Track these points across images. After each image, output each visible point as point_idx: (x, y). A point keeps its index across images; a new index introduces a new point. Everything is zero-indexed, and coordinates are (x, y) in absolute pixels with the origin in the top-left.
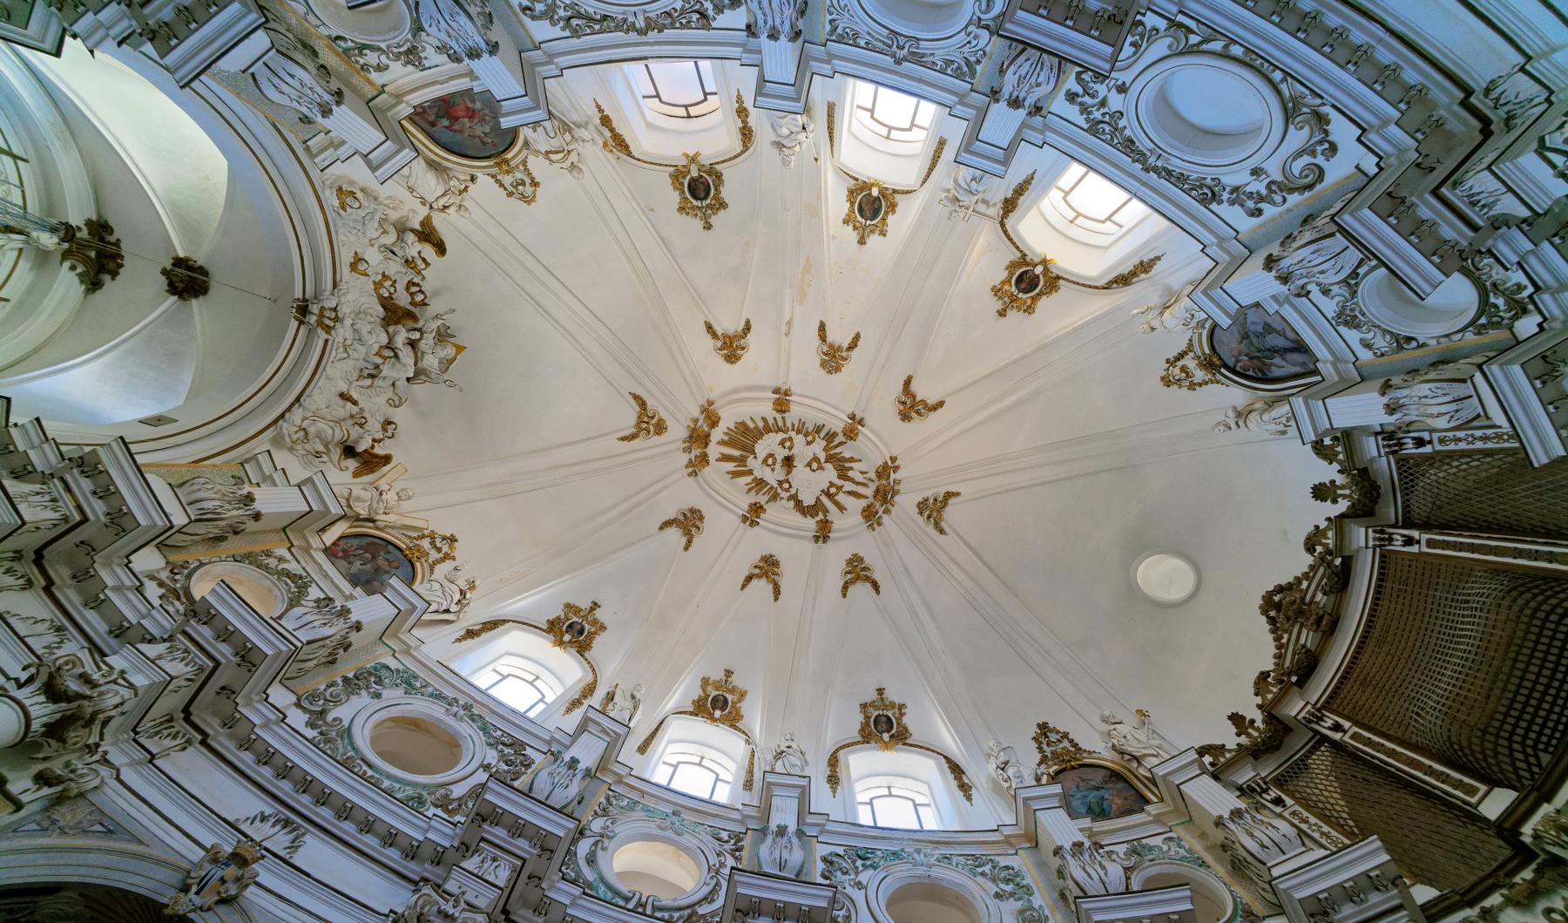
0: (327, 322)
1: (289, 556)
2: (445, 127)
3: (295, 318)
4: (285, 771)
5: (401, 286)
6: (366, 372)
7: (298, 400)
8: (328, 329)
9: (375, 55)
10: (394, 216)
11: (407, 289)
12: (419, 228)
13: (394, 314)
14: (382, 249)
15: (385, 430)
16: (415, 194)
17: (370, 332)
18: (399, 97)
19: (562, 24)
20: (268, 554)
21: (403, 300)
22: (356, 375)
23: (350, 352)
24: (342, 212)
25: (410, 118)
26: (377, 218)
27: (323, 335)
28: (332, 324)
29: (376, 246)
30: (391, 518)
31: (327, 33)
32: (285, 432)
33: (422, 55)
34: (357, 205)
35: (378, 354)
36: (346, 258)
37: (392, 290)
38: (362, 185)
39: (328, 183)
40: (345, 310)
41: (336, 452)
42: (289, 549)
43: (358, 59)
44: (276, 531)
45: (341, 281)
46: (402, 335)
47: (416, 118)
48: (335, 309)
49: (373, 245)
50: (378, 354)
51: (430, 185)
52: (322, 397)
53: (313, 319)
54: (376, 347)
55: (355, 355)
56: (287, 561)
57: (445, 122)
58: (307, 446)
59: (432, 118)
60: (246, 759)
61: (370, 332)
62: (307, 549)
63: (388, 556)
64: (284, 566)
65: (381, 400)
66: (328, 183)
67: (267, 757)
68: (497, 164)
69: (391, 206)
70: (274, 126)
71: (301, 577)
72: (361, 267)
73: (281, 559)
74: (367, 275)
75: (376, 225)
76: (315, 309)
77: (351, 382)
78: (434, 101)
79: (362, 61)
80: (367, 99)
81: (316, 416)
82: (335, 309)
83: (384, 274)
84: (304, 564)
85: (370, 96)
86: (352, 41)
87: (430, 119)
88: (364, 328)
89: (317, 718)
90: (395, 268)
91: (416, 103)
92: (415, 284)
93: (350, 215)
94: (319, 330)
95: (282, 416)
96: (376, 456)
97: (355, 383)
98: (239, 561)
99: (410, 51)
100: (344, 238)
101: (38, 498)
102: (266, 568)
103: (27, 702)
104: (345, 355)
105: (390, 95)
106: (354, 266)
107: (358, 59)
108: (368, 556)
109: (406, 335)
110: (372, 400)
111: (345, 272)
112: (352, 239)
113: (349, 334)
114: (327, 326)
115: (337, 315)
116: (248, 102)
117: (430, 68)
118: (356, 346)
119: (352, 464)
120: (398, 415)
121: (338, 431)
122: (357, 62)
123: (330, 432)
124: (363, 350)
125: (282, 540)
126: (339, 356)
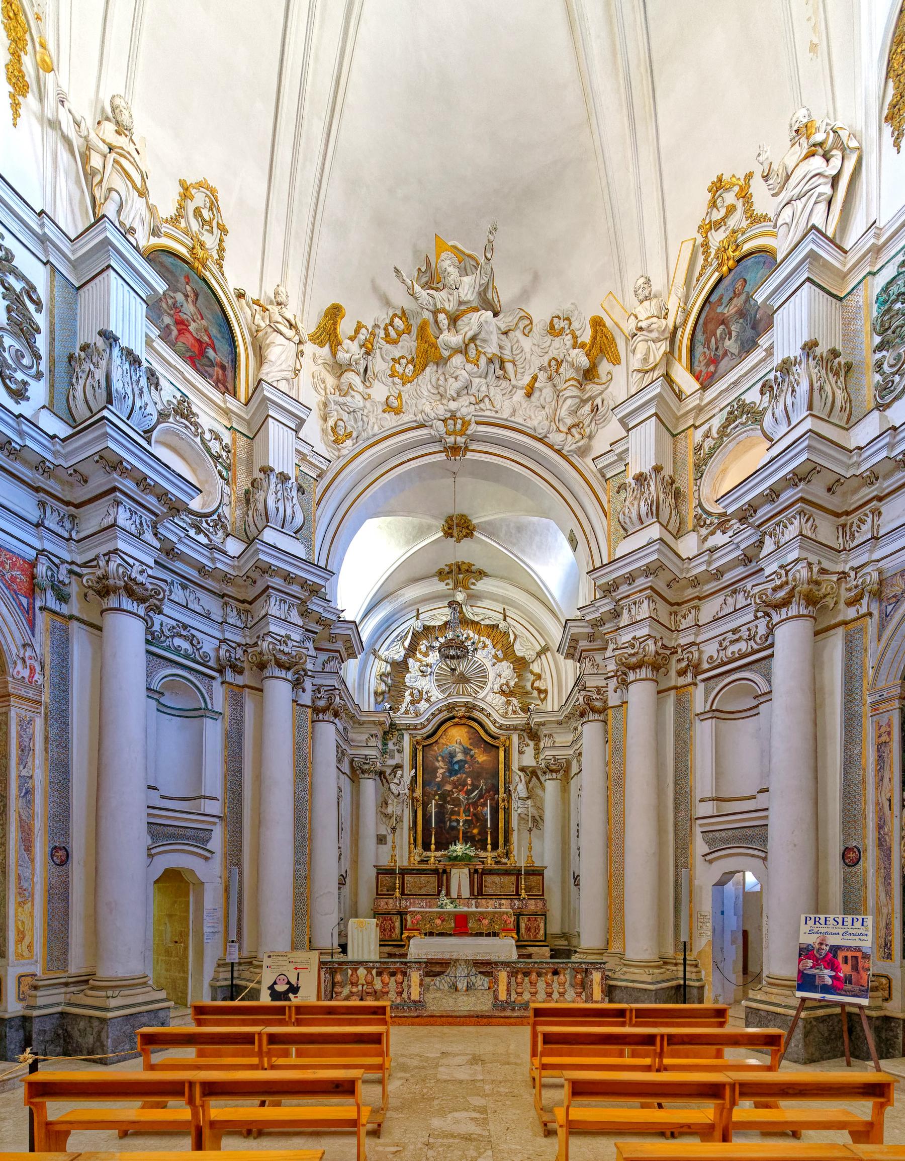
6: (499, 372)
17: (456, 378)
23: (482, 395)
24: (354, 435)
28: (459, 421)
45: (416, 421)
54: (469, 367)
61: (456, 378)
70: (318, 504)
77: (514, 387)
88: (453, 386)
97: (514, 382)
100: (376, 428)
104: (486, 400)
112: (372, 420)
113: (464, 401)
118: (473, 390)
126: (489, 407)
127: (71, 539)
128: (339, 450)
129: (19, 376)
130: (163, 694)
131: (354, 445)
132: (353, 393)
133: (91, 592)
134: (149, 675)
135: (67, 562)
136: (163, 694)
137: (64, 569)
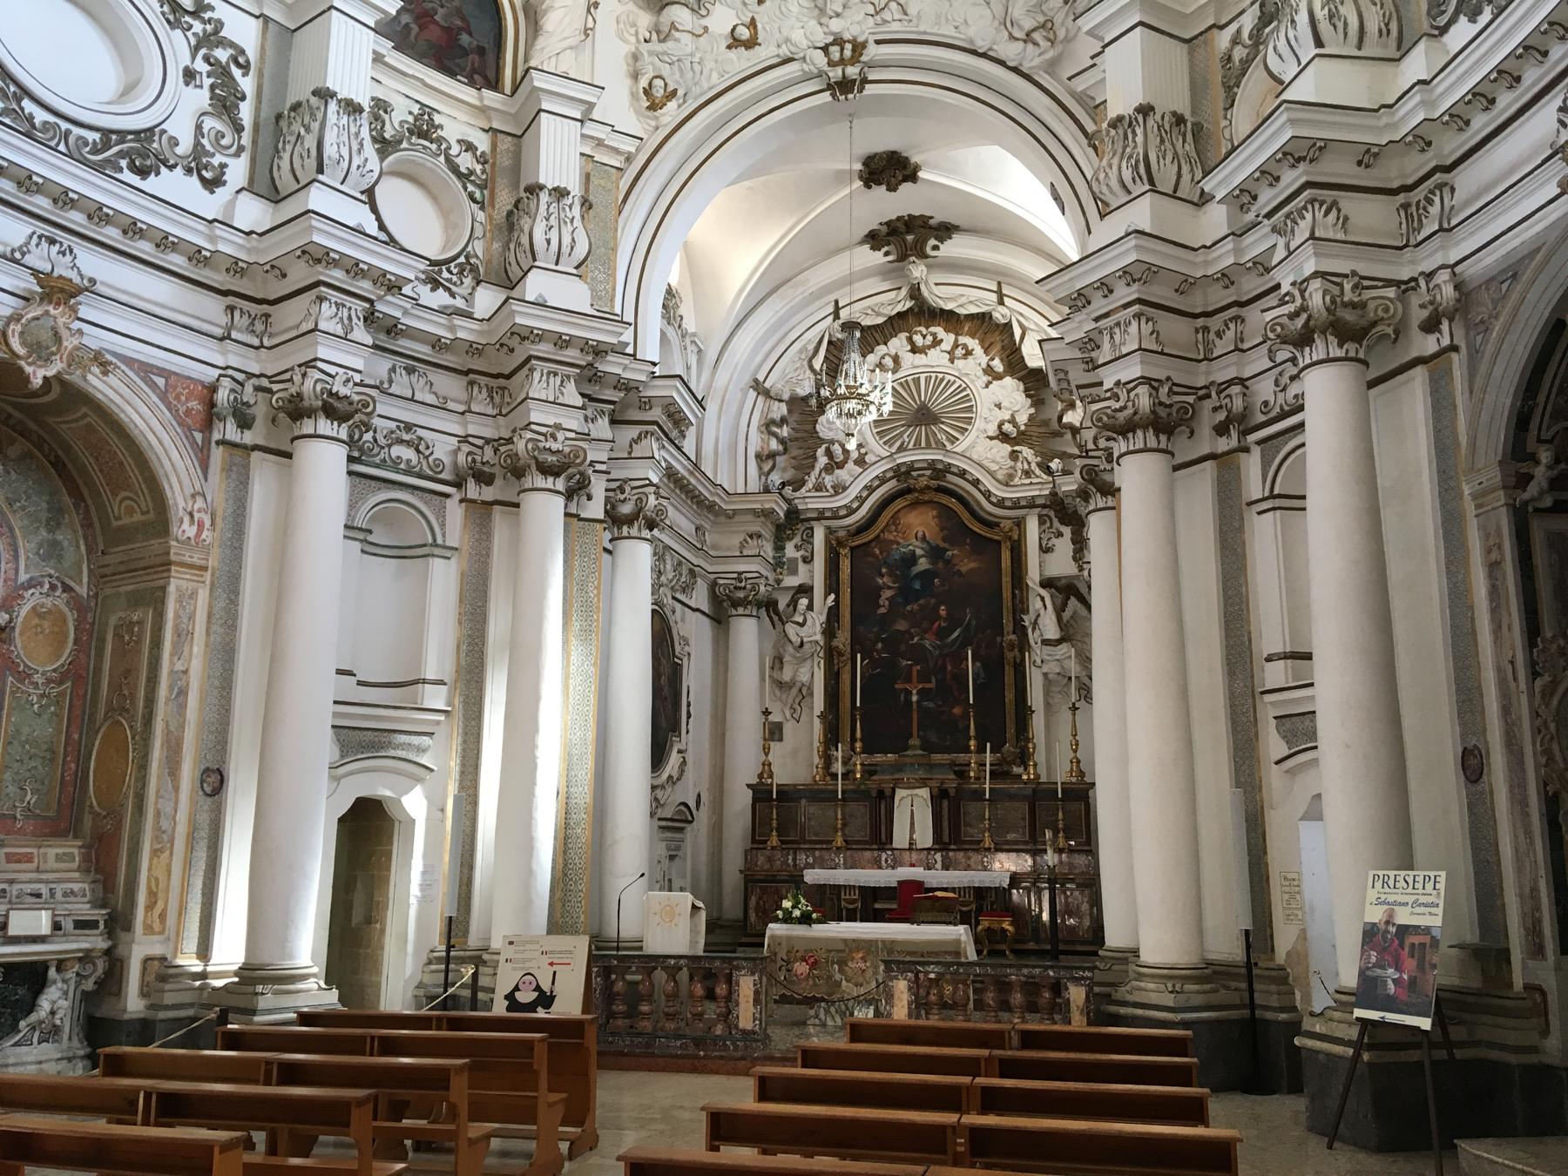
0: (848, 53)
1: (1233, 28)
2: (470, 34)
3: (861, 90)
7: (984, 55)
8: (858, 48)
9: (458, 160)
14: (703, 12)
16: (590, 24)
18: (483, 110)
19: (207, 15)
20: (1229, 58)
24: (680, 93)
25: (495, 85)
26: (659, 47)
27: (872, 52)
28: (849, 47)
29: (705, 22)
31: (481, 213)
32: (1037, 61)
33: (411, 119)
36: (742, 61)
38: (628, 82)
39: (653, 123)
42: (1222, 27)
43: (479, 172)
44: (1191, 53)
45: (778, 56)
47: (491, 74)
48: (825, 49)
49: (706, 29)
53: (852, 71)
56: (1239, 31)
57: (465, 39)
58: (1058, 20)
59: (474, 58)
60: (1482, 123)
64: (1245, 34)
66: (653, 123)
69: (633, 31)
72: (744, 33)
73: (1236, 40)
74: (753, 21)
75: (670, 44)
76: (836, 74)
78: (451, 73)
79: (478, 168)
80: (515, 140)
82: (825, 49)
85: (510, 139)
86: (465, 189)
87: (477, 58)
91: (473, 91)
93: (677, 82)
94: (864, 58)
95: (1015, 70)
98: (1233, 101)
99: (423, 135)
100: (715, 75)
101: (1117, 337)
103: (1308, 361)
105: (489, 119)
106: (751, 44)
107: (479, 172)
111: (765, 53)
112: (709, 64)
114: (853, 50)
115: (832, 44)
116: (615, 237)
117: (417, 101)
122: (483, 172)
125: (1205, 43)
127: (262, 346)
128: (657, 118)
129: (216, 160)
130: (370, 532)
131: (679, 106)
132: (677, 35)
133: (281, 415)
134: (353, 506)
135: (254, 375)
136: (370, 532)
137: (249, 388)
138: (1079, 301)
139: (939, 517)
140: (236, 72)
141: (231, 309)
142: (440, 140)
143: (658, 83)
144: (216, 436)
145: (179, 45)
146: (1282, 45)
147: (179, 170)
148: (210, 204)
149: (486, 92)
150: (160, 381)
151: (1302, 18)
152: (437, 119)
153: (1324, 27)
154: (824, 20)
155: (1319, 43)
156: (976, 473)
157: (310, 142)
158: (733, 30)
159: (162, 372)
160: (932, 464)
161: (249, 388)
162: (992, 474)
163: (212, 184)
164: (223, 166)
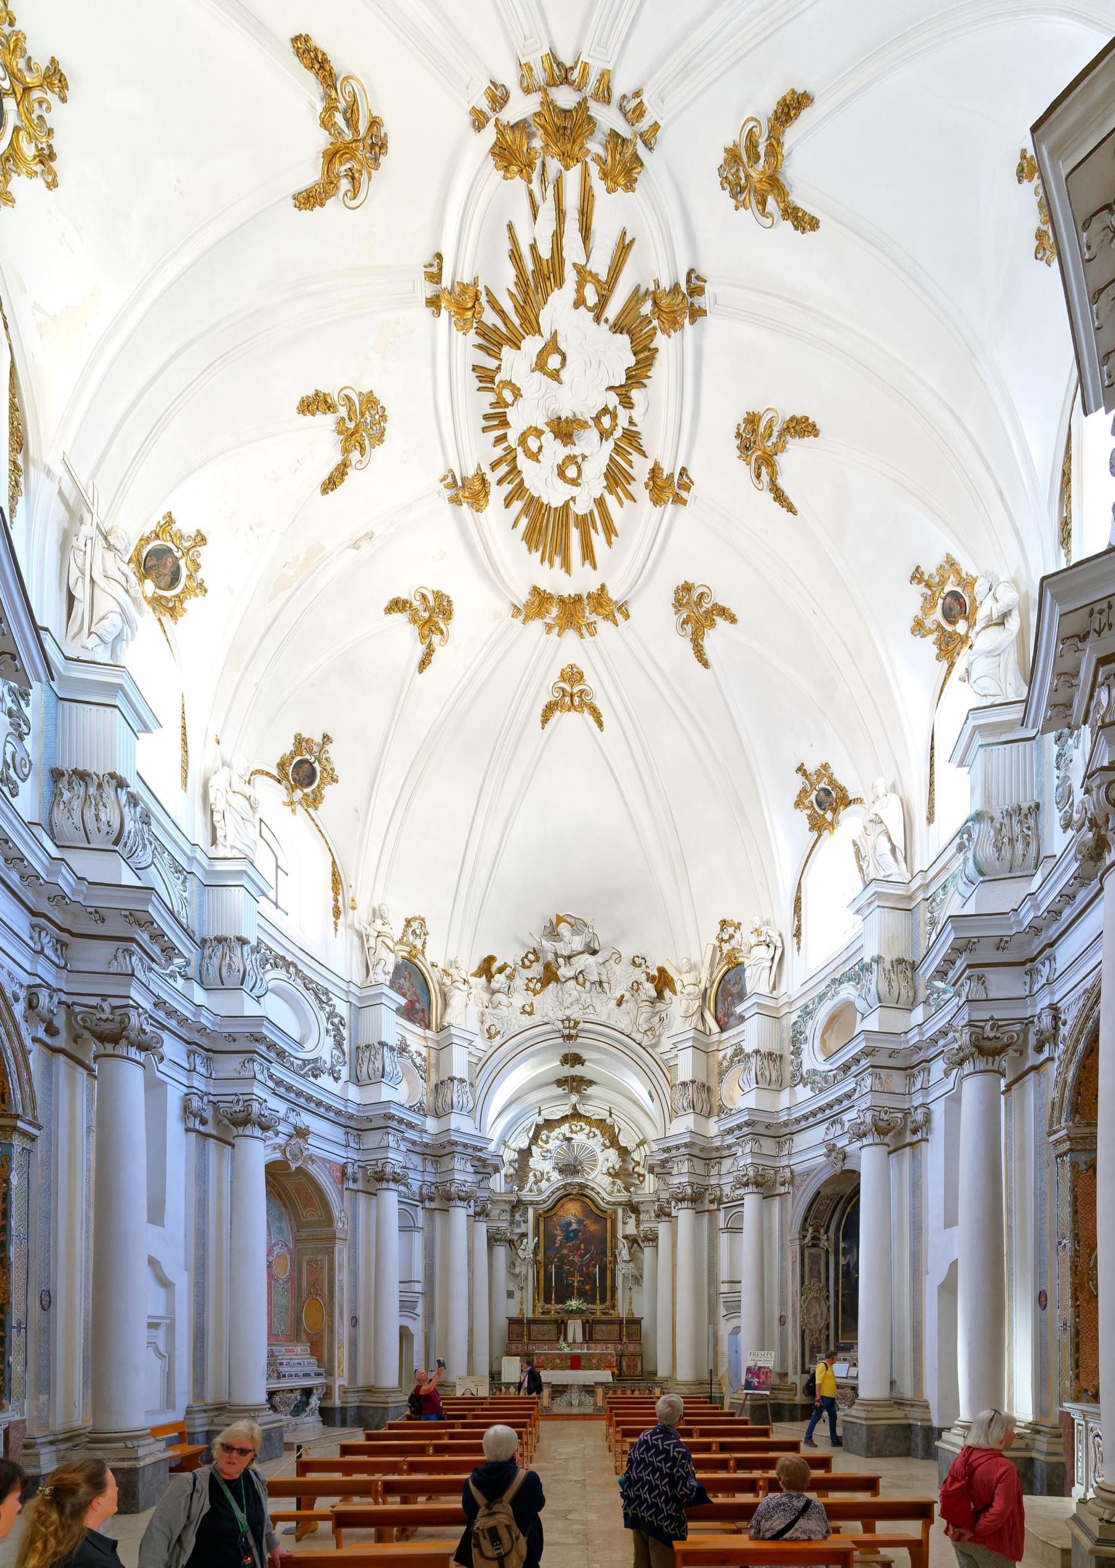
4: (814, 1114)
5: (529, 973)
8: (576, 1023)
10: (486, 996)
11: (529, 967)
12: (484, 977)
13: (550, 976)
15: (640, 966)
21: (537, 970)
22: (603, 996)
25: (428, 1026)
26: (493, 1011)
27: (581, 1026)
28: (572, 1022)
29: (511, 1000)
30: (704, 976)
34: (493, 1027)
35: (583, 985)
36: (526, 1021)
37: (535, 981)
40: (561, 1016)
41: (660, 1006)
46: (564, 971)
47: (427, 1021)
48: (563, 1021)
50: (583, 985)
51: (457, 999)
52: (622, 1019)
53: (573, 1032)
54: (579, 988)
55: (589, 1000)
57: (417, 1005)
58: (657, 1027)
62: (720, 1042)
63: (732, 982)
65: (616, 968)
67: (805, 1117)
68: (415, 957)
71: (736, 1050)
72: (528, 1009)
74: (532, 1003)
75: (497, 1011)
76: (566, 1032)
78: (414, 1023)
81: (635, 1023)
82: (563, 1021)
83: (526, 990)
84: (729, 1045)
89: (803, 1081)
90: (519, 982)
92: (523, 963)
96: (660, 978)
97: (609, 995)
102: (729, 1068)
104: (591, 1007)
106: (530, 1013)
108: (730, 999)
109: (563, 968)
110: (618, 978)
111: (537, 1019)
112: (514, 1021)
113: (575, 1008)
118: (582, 1001)
119: (667, 993)
120: (627, 954)
121: (643, 1009)
123: (645, 1015)
124: (583, 996)
138: (668, 1150)
139: (581, 1206)
140: (341, 1028)
141: (347, 1133)
142: (410, 1051)
143: (493, 1027)
144: (345, 1186)
145: (323, 1016)
146: (745, 1078)
147: (326, 1074)
148: (336, 1088)
149: (427, 1031)
150: (328, 1165)
151: (753, 1073)
152: (408, 1042)
153: (759, 1078)
154: (562, 1009)
155: (757, 1083)
156: (599, 1189)
157: (378, 1064)
158: (524, 1006)
159: (329, 1162)
160: (580, 1184)
161: (356, 1167)
162: (604, 1189)
163: (336, 1079)
164: (340, 1070)
